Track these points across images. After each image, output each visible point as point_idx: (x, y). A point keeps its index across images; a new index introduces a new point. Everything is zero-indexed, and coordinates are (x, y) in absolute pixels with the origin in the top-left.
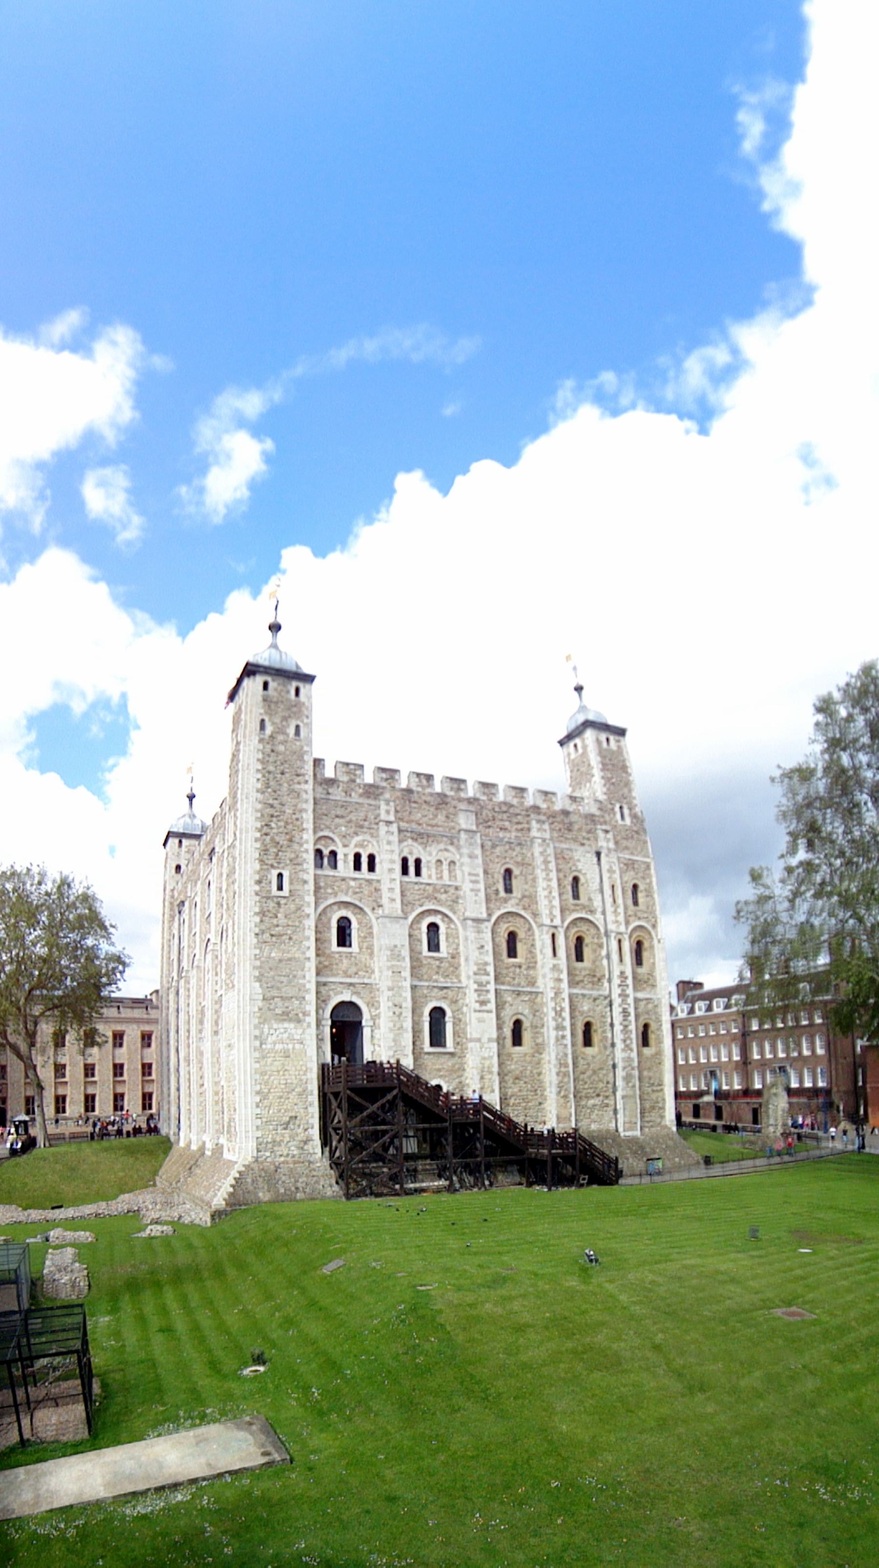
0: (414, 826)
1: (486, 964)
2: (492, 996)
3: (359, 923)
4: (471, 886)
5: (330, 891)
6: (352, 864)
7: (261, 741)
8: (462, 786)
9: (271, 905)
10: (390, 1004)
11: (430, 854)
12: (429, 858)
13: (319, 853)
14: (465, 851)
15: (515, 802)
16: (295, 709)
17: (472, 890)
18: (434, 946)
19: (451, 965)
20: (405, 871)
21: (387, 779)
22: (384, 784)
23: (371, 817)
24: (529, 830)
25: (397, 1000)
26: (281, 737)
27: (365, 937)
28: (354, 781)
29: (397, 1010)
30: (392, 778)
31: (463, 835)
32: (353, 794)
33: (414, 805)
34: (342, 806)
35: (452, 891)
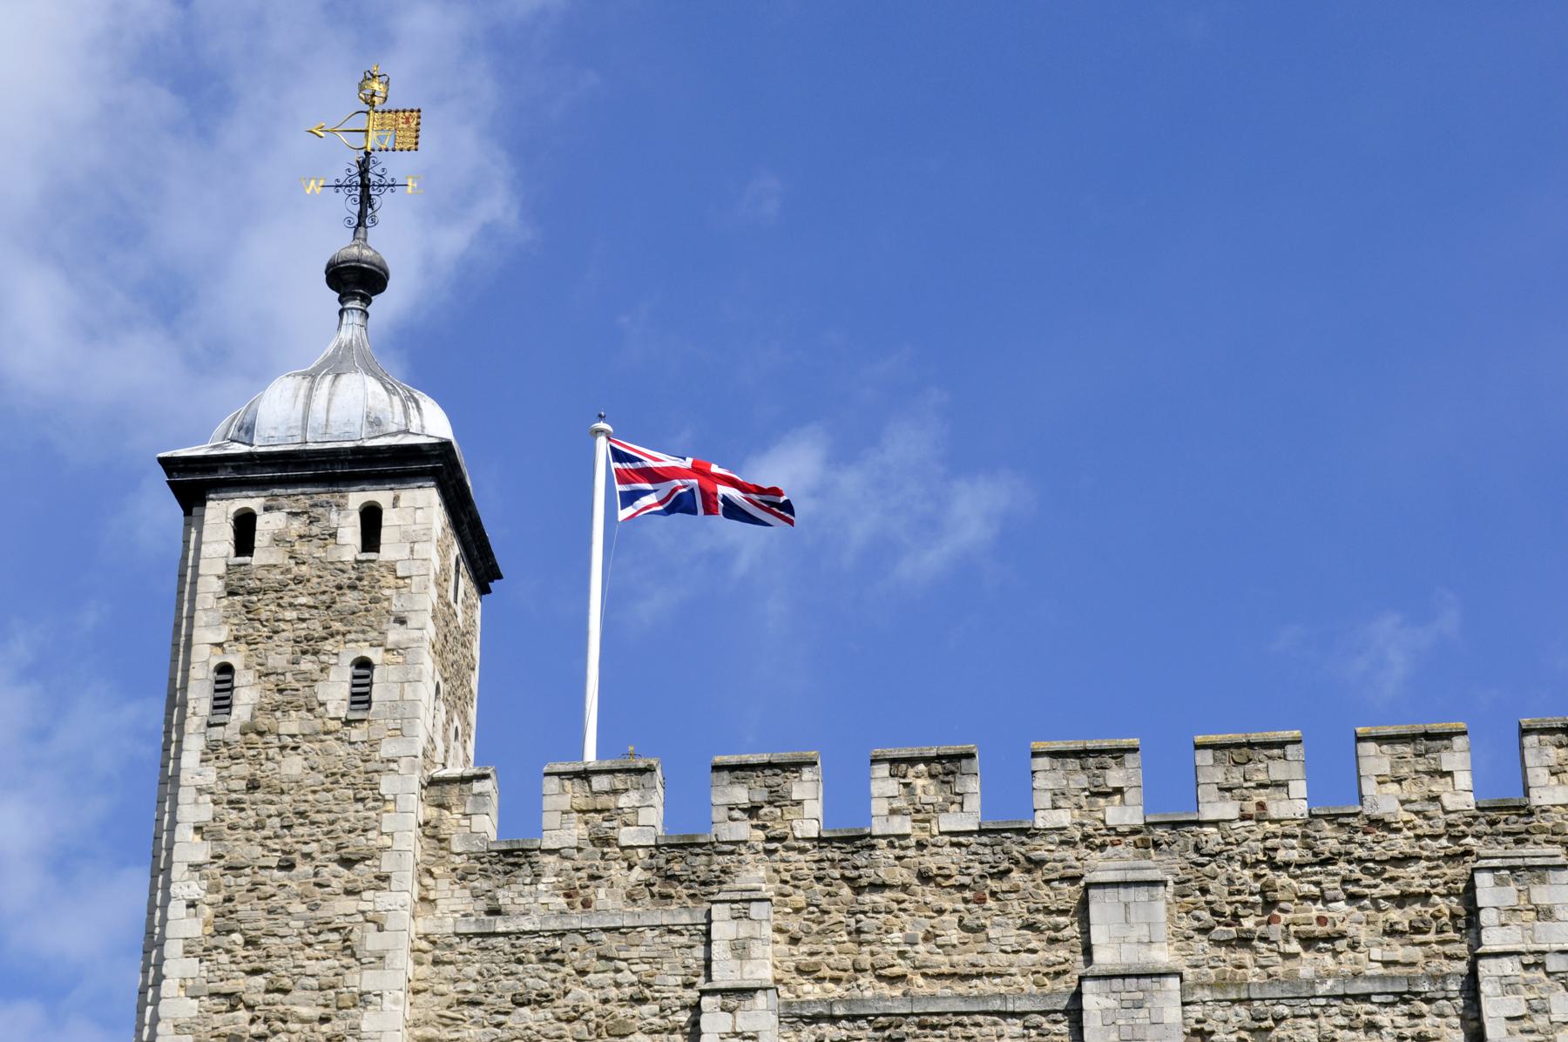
0: (869, 988)
7: (212, 750)
8: (1114, 778)
15: (1384, 801)
16: (351, 599)
21: (752, 811)
22: (743, 829)
23: (670, 981)
24: (1470, 919)
26: (291, 724)
28: (604, 841)
30: (777, 798)
32: (601, 895)
33: (867, 898)
34: (546, 956)
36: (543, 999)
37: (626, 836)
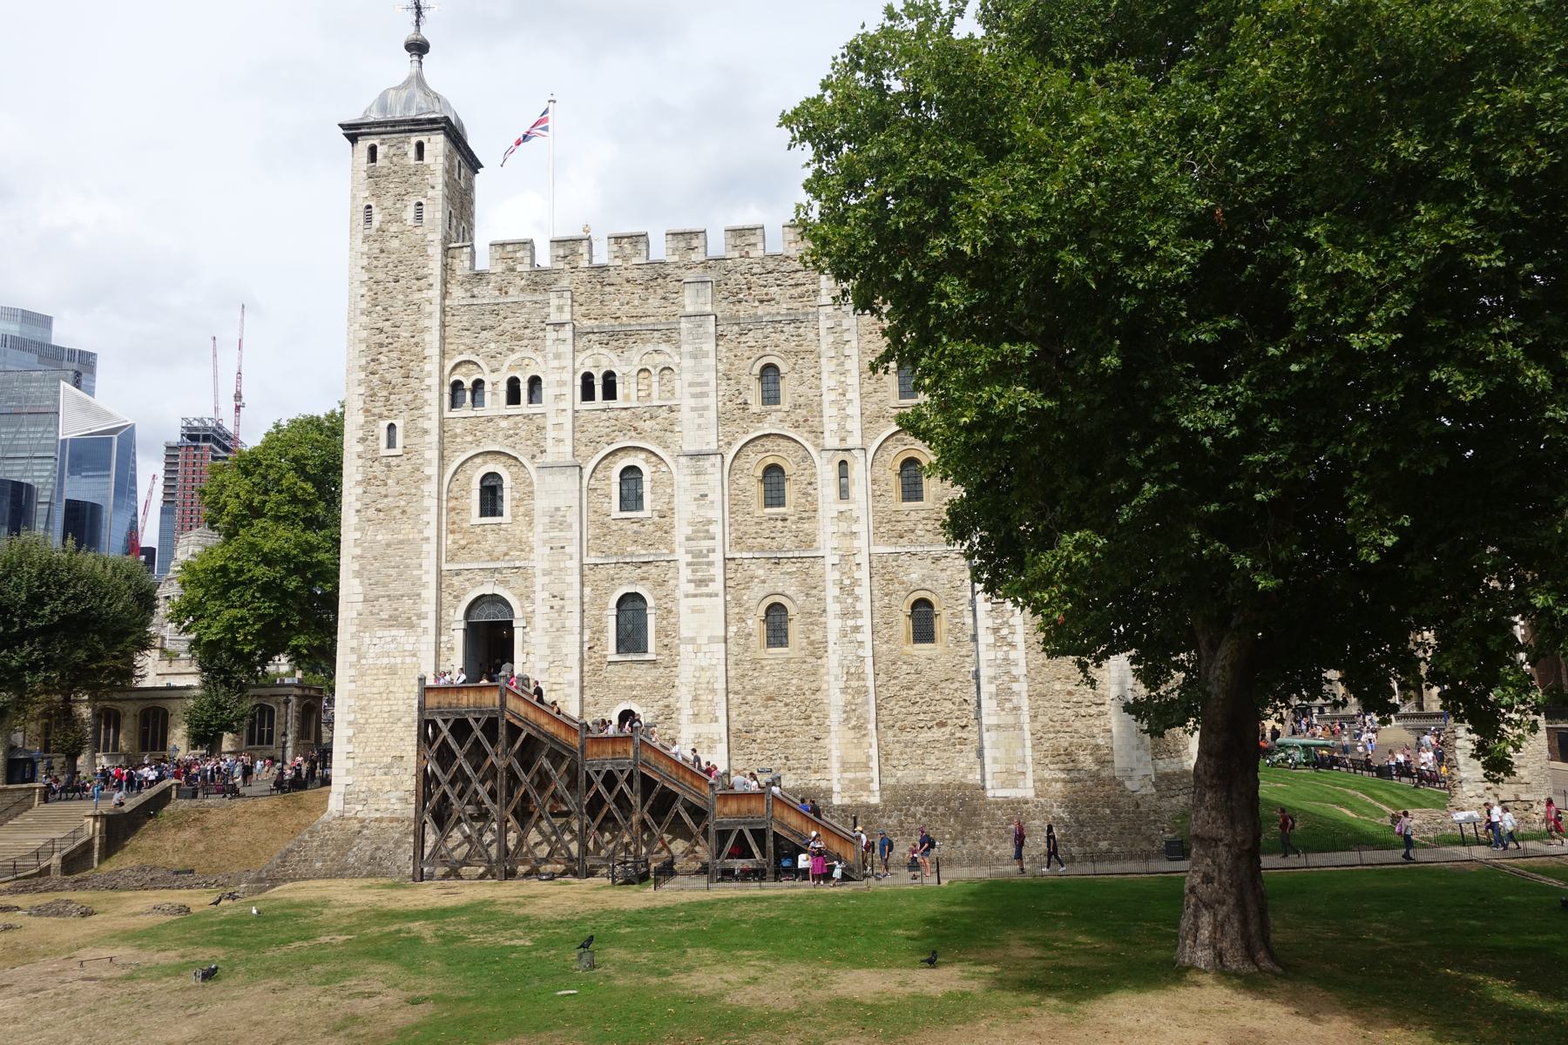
1: (710, 522)
2: (717, 571)
3: (515, 479)
4: (692, 402)
5: (469, 438)
6: (503, 396)
9: (378, 468)
10: (546, 595)
11: (629, 362)
12: (625, 369)
13: (457, 386)
14: (685, 348)
17: (693, 409)
18: (631, 498)
19: (658, 527)
20: (588, 394)
25: (556, 589)
27: (522, 499)
28: (513, 270)
29: (557, 603)
31: (685, 325)
32: (511, 290)
35: (663, 413)
36: (492, 328)
37: (519, 268)
